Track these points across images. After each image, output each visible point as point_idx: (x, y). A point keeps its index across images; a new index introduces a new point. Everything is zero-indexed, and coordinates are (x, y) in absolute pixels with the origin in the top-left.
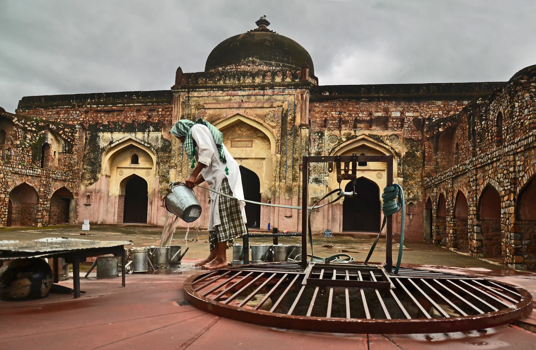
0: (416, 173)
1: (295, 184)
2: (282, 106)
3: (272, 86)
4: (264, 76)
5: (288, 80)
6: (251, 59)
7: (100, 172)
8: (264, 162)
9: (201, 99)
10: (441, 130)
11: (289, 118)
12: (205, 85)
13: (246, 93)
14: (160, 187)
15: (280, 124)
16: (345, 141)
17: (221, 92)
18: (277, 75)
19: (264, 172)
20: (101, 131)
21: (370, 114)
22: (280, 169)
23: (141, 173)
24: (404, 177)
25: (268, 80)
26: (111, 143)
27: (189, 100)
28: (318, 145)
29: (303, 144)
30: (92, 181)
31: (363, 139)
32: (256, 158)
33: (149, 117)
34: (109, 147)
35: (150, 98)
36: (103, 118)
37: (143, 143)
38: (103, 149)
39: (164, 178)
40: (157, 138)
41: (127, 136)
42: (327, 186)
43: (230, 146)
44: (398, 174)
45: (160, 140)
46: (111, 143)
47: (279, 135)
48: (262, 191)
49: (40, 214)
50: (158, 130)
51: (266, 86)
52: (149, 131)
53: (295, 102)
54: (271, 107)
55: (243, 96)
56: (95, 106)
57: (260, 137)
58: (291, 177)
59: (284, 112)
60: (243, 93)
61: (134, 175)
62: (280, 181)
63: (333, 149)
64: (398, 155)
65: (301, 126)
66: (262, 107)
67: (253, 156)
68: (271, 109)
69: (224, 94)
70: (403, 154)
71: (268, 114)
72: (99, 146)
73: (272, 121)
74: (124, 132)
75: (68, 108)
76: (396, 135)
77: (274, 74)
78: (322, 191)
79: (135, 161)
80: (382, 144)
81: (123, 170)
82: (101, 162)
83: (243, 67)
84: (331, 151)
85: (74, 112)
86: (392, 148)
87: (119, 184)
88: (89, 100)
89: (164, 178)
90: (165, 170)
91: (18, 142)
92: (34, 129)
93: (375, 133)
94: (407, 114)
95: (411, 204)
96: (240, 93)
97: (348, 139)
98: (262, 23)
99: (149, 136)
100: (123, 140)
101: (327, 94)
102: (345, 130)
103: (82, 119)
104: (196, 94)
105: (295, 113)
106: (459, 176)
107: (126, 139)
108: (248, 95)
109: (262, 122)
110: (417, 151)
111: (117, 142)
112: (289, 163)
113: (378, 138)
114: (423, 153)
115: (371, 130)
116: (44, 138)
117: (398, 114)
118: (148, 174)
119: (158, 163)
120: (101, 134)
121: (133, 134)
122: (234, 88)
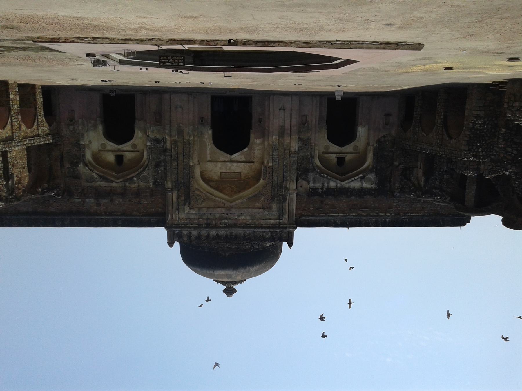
0: (69, 149)
1: (176, 138)
2: (190, 209)
3: (200, 226)
4: (208, 235)
5: (185, 232)
6: (227, 254)
7: (375, 149)
8: (209, 158)
9: (267, 217)
10: (46, 185)
11: (182, 198)
12: (264, 230)
13: (223, 221)
14: (309, 135)
15: (191, 193)
16: (133, 177)
17: (248, 223)
18: (196, 237)
19: (208, 149)
20: (375, 190)
21: (112, 201)
22: (190, 152)
23: (334, 148)
24: (79, 144)
25: (204, 232)
26: (362, 178)
27: (279, 216)
28: (158, 173)
29: (169, 174)
30: (383, 139)
31: (118, 179)
32: (217, 162)
33: (322, 202)
34: (364, 174)
35: (322, 220)
36: (372, 202)
37: (329, 177)
38: (371, 171)
39: (305, 143)
40: (314, 182)
41: (345, 184)
42: (148, 136)
43: (242, 174)
44: (84, 148)
45: (311, 179)
46: (362, 178)
47: (192, 183)
48: (210, 132)
49: (420, 105)
50: (313, 189)
51: (205, 227)
52: (322, 189)
53: (179, 212)
54: (200, 209)
55: (226, 219)
56: (381, 214)
57: (214, 182)
58: (179, 144)
59: (187, 203)
60: (226, 221)
61: (341, 146)
62: (188, 140)
63: (144, 170)
64: (86, 165)
65: (172, 190)
66: (208, 208)
67: (219, 165)
68: (200, 206)
69: (244, 221)
70: (81, 165)
71: (202, 202)
72: (376, 174)
73: (198, 195)
74: (349, 188)
75: (411, 213)
76: (89, 182)
77: (199, 237)
78: (153, 132)
79: (341, 160)
80: (100, 174)
81: (354, 151)
82: (374, 159)
83: (234, 247)
84: (146, 168)
85: (404, 209)
86: (91, 170)
87: (358, 137)
88: (388, 220)
89: (305, 143)
90: (305, 151)
91: (445, 176)
92: (434, 190)
93: (106, 184)
94: (80, 200)
95: (71, 121)
96: (230, 221)
97: (131, 179)
98: (230, 291)
99: (323, 184)
100: (350, 180)
101: (152, 220)
102: (134, 187)
103: (395, 201)
104: (272, 221)
105: (178, 203)
106: (3, 142)
107: (347, 181)
108: (223, 219)
109: (208, 195)
110: (68, 167)
111: (356, 178)
112: (181, 158)
113: (104, 178)
114: (62, 166)
115: (111, 187)
116: (426, 181)
117: (87, 200)
118: (327, 147)
119: (313, 157)
120: (374, 186)
121: (339, 185)
122: (235, 226)
